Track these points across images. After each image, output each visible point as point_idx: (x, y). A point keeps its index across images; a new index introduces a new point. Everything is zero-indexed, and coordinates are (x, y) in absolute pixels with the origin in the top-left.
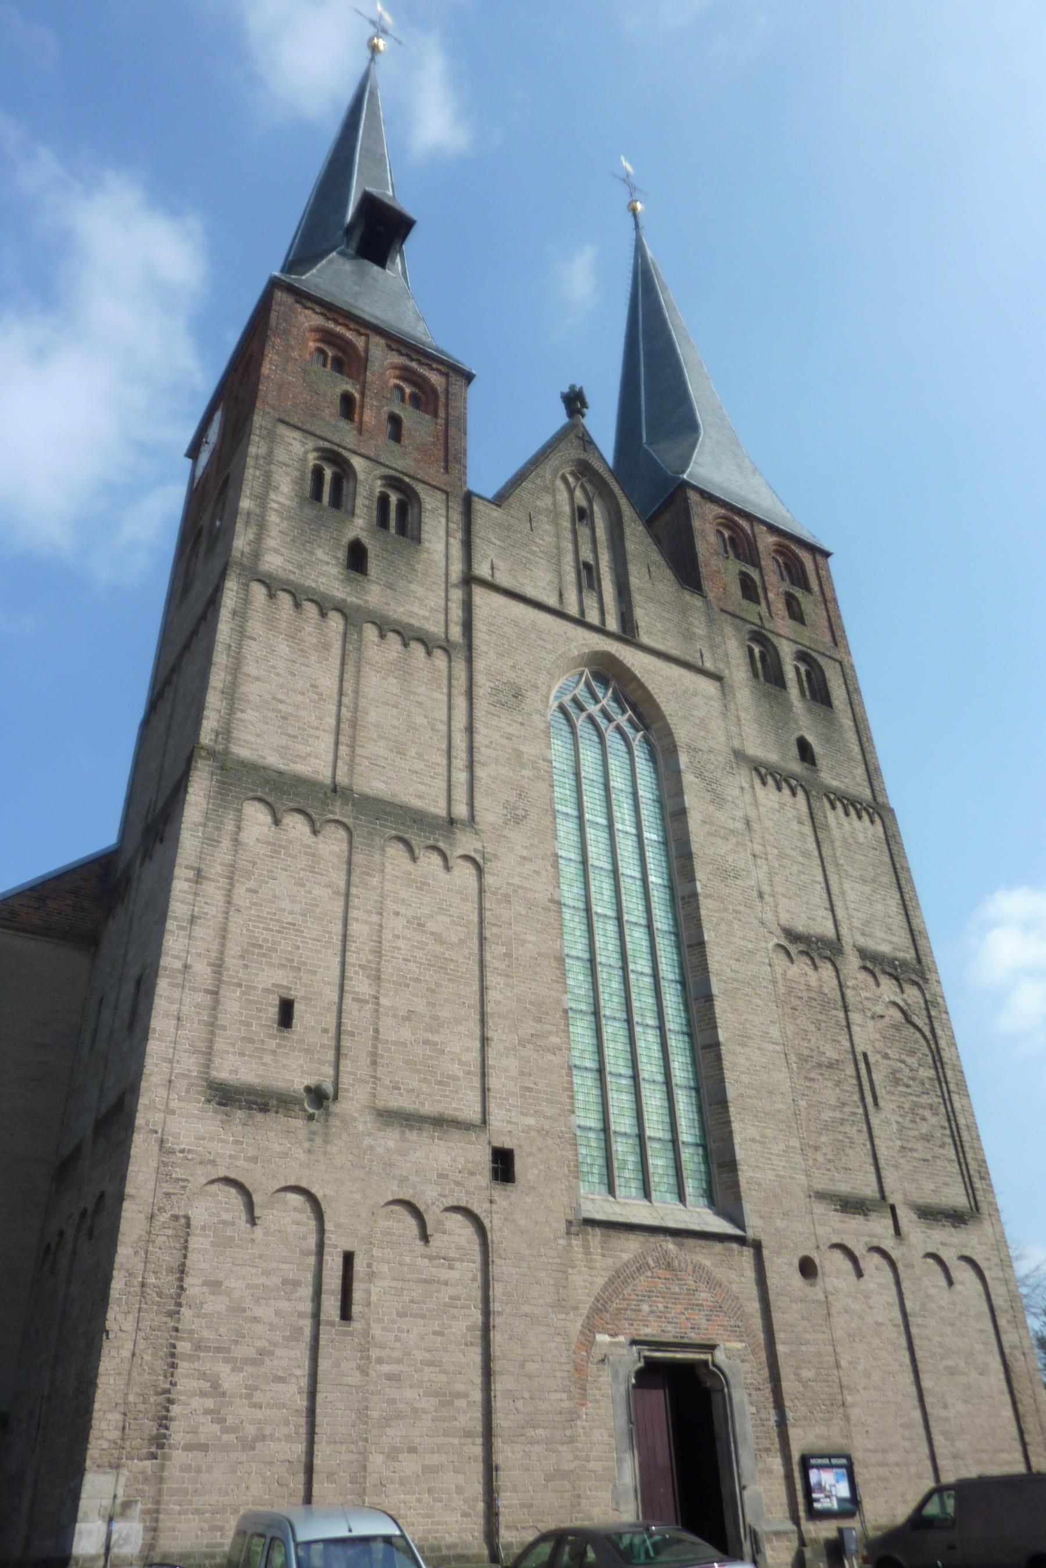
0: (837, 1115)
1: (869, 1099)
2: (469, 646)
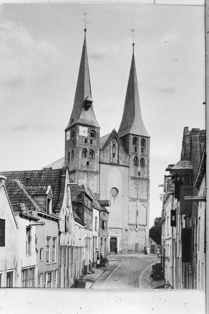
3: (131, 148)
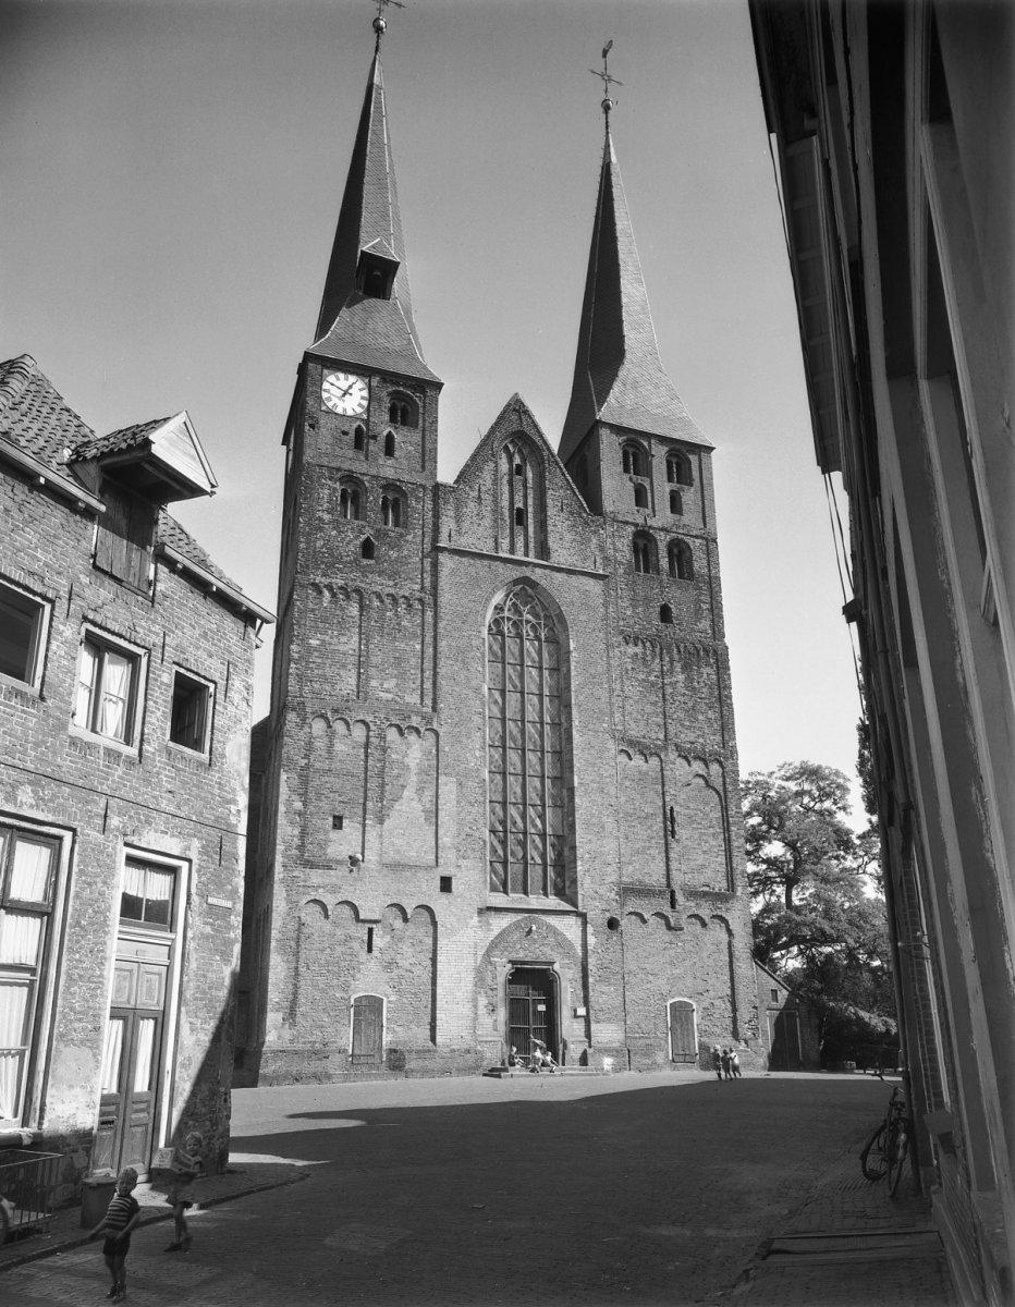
0: (648, 844)
3: (615, 485)
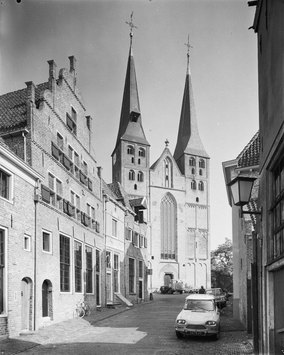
1: (196, 248)
2: (150, 197)
